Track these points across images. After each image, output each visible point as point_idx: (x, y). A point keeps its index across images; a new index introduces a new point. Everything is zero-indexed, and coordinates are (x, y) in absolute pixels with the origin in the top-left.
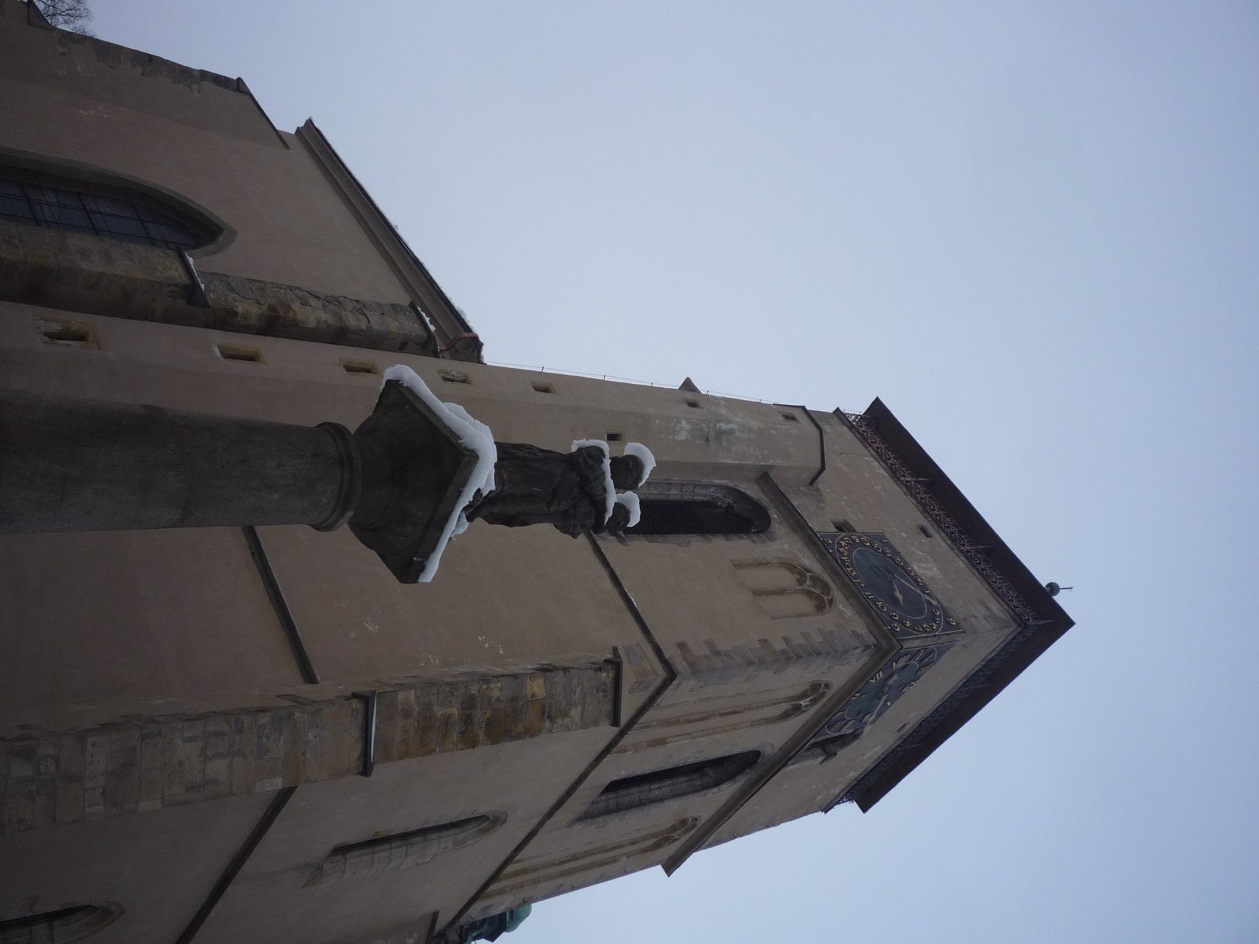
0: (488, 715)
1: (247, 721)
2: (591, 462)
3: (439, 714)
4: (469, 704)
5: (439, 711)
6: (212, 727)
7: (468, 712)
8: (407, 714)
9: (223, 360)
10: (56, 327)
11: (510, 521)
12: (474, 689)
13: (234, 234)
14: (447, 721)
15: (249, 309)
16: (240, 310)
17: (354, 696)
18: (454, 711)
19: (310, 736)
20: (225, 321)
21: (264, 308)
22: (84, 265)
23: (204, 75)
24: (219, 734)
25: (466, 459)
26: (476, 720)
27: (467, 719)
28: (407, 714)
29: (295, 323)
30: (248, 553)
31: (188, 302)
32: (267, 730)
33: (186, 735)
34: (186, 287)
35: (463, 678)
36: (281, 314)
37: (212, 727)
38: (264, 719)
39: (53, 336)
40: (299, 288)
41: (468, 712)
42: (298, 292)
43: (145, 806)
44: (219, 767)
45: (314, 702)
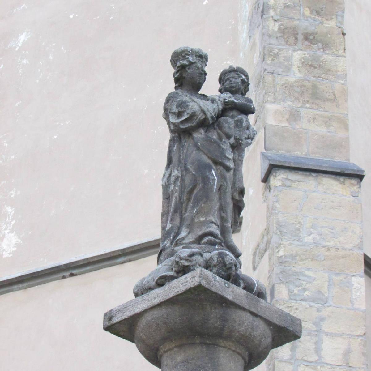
0: (307, 12)
2: (185, 117)
3: (298, 75)
4: (290, 35)
5: (296, 75)
7: (300, 37)
8: (294, 116)
11: (238, 207)
12: (274, 27)
14: (310, 65)
17: (265, 180)
18: (297, 56)
19: (309, 239)
25: (204, 283)
26: (312, 29)
27: (309, 38)
28: (294, 116)
30: (69, 281)
32: (296, 290)
35: (257, 36)
41: (300, 37)
45: (267, 230)
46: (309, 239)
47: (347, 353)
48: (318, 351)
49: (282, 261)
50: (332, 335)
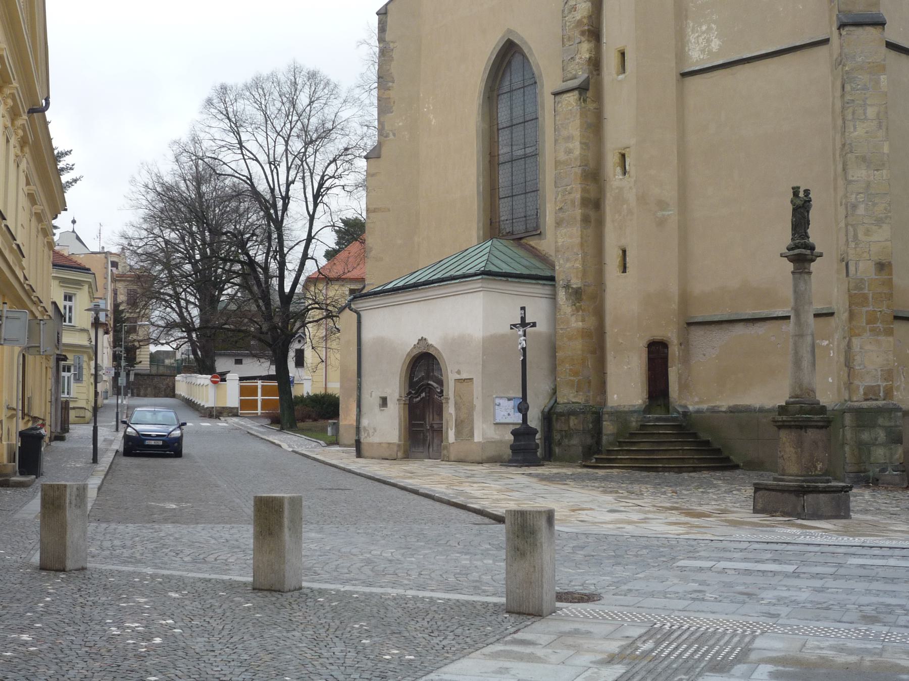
1: (848, 97)
6: (850, 117)
9: (627, 73)
10: (619, 170)
13: (510, 31)
15: (585, 50)
16: (588, 56)
20: (596, 64)
21: (583, 39)
22: (577, 152)
23: (381, 40)
24: (853, 113)
29: (590, 17)
31: (587, 90)
33: (852, 130)
34: (580, 94)
36: (586, 28)
37: (850, 117)
38: (848, 88)
39: (625, 172)
40: (563, 11)
42: (566, 12)
43: (886, 149)
44: (871, 112)
46: (860, 60)
47: (878, 114)
48: (865, 114)
49: (847, 72)
50: (871, 105)
